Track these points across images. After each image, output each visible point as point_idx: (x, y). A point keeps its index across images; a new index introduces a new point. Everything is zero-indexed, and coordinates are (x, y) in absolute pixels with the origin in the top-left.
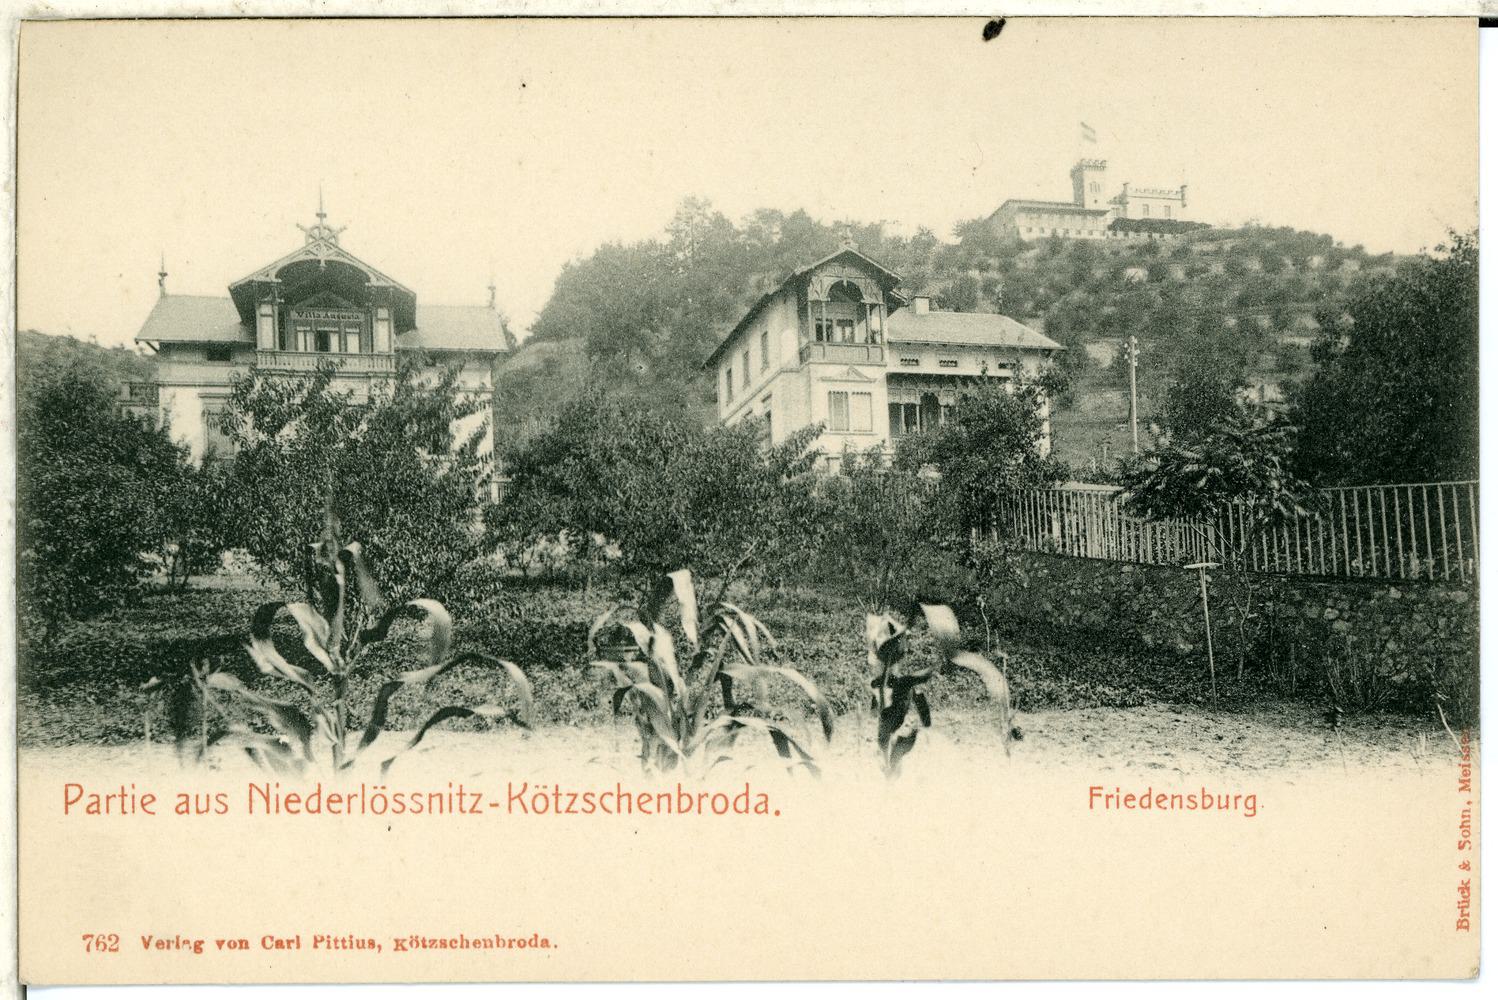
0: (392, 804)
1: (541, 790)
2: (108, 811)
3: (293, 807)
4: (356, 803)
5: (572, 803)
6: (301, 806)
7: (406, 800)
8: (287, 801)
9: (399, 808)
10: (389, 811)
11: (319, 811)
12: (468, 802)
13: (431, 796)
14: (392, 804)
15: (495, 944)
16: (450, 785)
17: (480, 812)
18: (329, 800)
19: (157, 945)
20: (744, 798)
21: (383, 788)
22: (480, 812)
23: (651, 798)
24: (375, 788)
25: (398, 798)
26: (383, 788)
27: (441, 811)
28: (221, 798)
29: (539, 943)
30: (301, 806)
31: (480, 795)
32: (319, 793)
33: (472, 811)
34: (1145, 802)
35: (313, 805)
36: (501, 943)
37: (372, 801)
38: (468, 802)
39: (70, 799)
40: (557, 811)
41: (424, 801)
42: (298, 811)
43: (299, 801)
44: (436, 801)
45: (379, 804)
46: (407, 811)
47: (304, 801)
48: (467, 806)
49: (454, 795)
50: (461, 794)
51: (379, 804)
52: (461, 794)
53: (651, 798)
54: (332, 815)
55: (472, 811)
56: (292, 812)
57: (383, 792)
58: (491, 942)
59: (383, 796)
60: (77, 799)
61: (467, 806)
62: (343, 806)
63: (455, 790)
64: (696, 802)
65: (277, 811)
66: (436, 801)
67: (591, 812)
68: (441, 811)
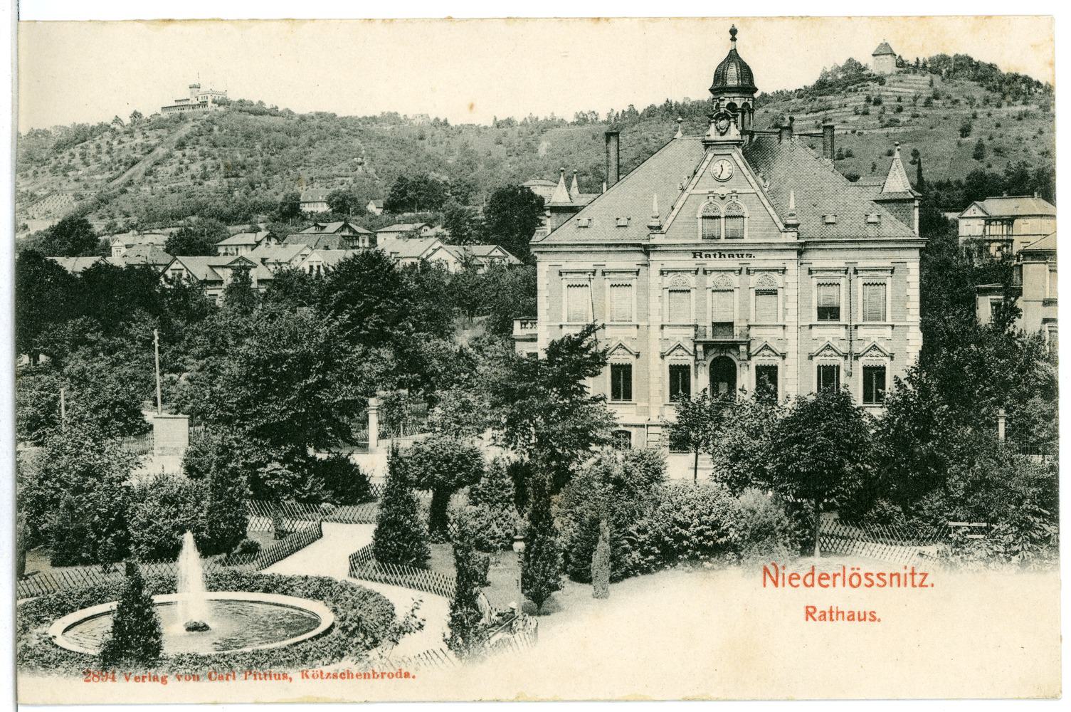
0: (864, 581)
1: (856, 571)
3: (794, 582)
4: (839, 580)
5: (924, 578)
6: (800, 582)
7: (874, 578)
8: (790, 579)
9: (868, 583)
11: (812, 585)
12: (918, 579)
13: (892, 575)
14: (864, 581)
15: (372, 676)
16: (906, 568)
18: (820, 578)
19: (357, 676)
20: (810, 577)
21: (858, 569)
22: (927, 586)
24: (853, 569)
25: (869, 576)
26: (858, 569)
27: (899, 585)
29: (403, 675)
30: (800, 582)
31: (925, 575)
32: (813, 574)
33: (921, 585)
34: (809, 581)
35: (809, 581)
36: (376, 676)
37: (851, 577)
38: (918, 579)
39: (810, 577)
40: (913, 585)
41: (887, 578)
42: (798, 586)
43: (799, 578)
44: (895, 578)
45: (855, 580)
47: (802, 576)
48: (917, 582)
50: (913, 574)
51: (855, 580)
52: (913, 574)
54: (822, 588)
56: (795, 587)
57: (857, 571)
58: (369, 675)
59: (856, 574)
60: (807, 575)
61: (917, 582)
62: (830, 582)
63: (909, 571)
64: (847, 582)
65: (784, 585)
66: (895, 578)
67: (880, 586)
68: (899, 585)
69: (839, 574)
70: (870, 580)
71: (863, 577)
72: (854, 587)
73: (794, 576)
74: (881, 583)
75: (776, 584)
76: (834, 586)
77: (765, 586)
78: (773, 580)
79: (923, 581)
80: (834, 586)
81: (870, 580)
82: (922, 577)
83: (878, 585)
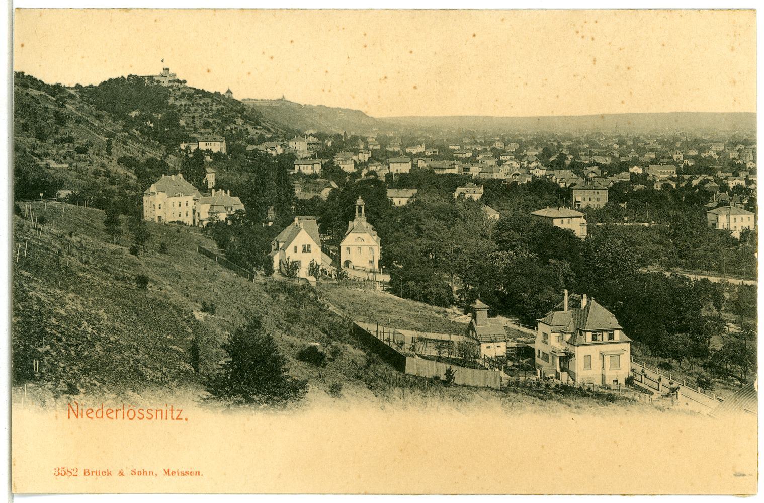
0: (138, 415)
2: (167, 419)
7: (146, 415)
9: (141, 416)
10: (136, 416)
11: (102, 417)
12: (175, 414)
14: (138, 415)
17: (181, 419)
22: (181, 419)
23: (113, 412)
25: (141, 411)
28: (141, 411)
33: (177, 418)
35: (99, 415)
38: (175, 414)
41: (154, 413)
44: (159, 413)
46: (145, 418)
47: (95, 412)
48: (175, 415)
49: (168, 411)
53: (93, 412)
55: (177, 418)
66: (159, 413)
68: (162, 418)
69: (120, 410)
70: (141, 414)
71: (136, 411)
72: (130, 419)
73: (90, 411)
74: (150, 416)
75: (77, 417)
76: (116, 418)
77: (69, 418)
78: (75, 415)
79: (178, 416)
80: (116, 418)
81: (141, 414)
82: (179, 412)
83: (147, 418)
